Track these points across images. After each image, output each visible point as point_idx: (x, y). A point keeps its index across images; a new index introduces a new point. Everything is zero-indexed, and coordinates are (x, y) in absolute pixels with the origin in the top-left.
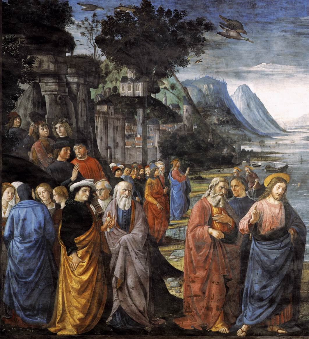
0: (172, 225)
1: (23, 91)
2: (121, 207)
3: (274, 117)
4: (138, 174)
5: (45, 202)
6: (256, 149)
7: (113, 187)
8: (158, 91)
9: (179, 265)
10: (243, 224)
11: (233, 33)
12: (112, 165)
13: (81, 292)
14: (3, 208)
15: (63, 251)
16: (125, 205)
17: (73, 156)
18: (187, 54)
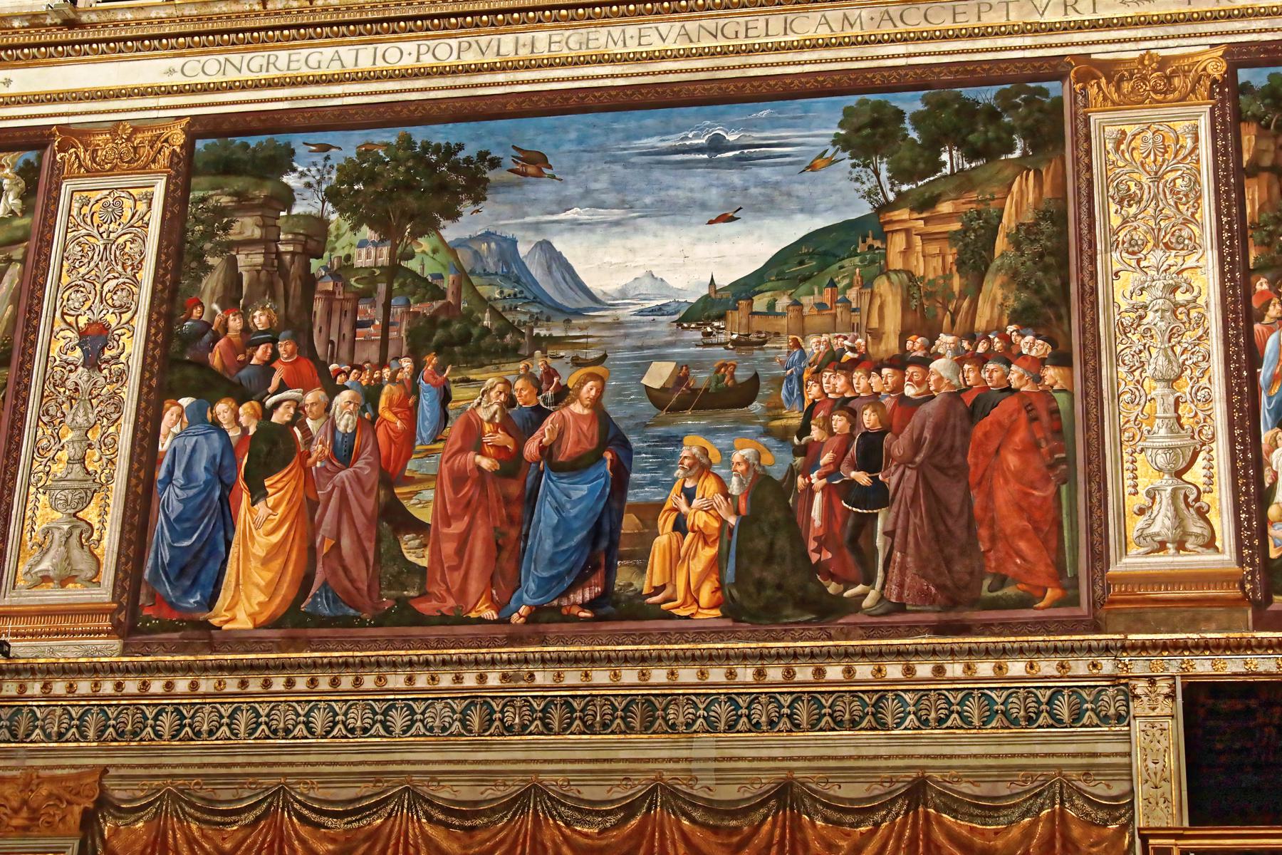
0: (418, 453)
1: (211, 268)
2: (341, 428)
3: (588, 285)
4: (371, 377)
5: (226, 427)
6: (557, 333)
7: (332, 399)
8: (411, 256)
9: (425, 515)
10: (531, 448)
11: (531, 169)
12: (333, 367)
13: (266, 562)
14: (161, 438)
15: (245, 498)
16: (347, 426)
17: (275, 355)
18: (460, 202)
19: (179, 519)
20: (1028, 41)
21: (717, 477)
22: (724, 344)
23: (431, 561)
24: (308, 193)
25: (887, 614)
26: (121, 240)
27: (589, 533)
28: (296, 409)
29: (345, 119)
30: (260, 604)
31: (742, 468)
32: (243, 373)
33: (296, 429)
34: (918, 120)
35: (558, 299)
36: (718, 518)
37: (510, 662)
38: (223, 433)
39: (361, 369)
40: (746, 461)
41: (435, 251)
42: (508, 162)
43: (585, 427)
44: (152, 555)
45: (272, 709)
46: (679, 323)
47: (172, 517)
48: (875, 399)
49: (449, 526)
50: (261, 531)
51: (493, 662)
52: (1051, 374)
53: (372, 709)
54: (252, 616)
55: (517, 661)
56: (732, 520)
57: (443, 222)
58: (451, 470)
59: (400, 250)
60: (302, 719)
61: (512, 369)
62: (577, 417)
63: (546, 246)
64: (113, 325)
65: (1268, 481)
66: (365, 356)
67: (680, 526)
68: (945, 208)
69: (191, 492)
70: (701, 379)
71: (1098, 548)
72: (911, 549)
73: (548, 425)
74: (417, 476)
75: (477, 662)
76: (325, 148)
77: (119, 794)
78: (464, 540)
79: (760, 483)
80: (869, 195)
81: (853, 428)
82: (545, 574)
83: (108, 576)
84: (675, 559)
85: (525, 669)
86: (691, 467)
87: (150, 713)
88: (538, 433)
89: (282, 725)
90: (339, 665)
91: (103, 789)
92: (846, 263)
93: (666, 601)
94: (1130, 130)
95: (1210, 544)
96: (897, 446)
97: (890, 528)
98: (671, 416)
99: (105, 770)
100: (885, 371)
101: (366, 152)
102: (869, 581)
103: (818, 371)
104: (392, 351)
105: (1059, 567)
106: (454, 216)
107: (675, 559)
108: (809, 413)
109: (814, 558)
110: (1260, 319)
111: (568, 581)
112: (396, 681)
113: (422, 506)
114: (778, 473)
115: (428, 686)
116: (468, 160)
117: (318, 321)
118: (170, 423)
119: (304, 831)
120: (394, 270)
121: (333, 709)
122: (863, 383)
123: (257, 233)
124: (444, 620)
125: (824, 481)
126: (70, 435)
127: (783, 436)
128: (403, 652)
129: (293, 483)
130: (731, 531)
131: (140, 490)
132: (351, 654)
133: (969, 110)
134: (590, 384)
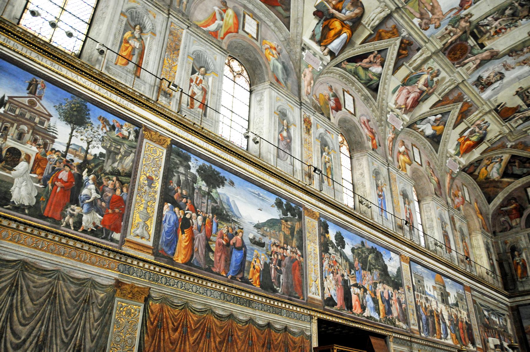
6: (236, 220)
9: (214, 249)
13: (184, 249)
19: (167, 232)
38: (176, 215)
46: (254, 227)
51: (227, 286)
52: (301, 258)
54: (182, 260)
63: (233, 201)
67: (254, 267)
70: (257, 239)
77: (153, 295)
83: (152, 239)
84: (254, 274)
85: (232, 289)
87: (160, 277)
91: (149, 293)
96: (283, 263)
99: (150, 288)
101: (204, 165)
114: (268, 263)
119: (191, 314)
123: (184, 172)
126: (144, 202)
127: (268, 255)
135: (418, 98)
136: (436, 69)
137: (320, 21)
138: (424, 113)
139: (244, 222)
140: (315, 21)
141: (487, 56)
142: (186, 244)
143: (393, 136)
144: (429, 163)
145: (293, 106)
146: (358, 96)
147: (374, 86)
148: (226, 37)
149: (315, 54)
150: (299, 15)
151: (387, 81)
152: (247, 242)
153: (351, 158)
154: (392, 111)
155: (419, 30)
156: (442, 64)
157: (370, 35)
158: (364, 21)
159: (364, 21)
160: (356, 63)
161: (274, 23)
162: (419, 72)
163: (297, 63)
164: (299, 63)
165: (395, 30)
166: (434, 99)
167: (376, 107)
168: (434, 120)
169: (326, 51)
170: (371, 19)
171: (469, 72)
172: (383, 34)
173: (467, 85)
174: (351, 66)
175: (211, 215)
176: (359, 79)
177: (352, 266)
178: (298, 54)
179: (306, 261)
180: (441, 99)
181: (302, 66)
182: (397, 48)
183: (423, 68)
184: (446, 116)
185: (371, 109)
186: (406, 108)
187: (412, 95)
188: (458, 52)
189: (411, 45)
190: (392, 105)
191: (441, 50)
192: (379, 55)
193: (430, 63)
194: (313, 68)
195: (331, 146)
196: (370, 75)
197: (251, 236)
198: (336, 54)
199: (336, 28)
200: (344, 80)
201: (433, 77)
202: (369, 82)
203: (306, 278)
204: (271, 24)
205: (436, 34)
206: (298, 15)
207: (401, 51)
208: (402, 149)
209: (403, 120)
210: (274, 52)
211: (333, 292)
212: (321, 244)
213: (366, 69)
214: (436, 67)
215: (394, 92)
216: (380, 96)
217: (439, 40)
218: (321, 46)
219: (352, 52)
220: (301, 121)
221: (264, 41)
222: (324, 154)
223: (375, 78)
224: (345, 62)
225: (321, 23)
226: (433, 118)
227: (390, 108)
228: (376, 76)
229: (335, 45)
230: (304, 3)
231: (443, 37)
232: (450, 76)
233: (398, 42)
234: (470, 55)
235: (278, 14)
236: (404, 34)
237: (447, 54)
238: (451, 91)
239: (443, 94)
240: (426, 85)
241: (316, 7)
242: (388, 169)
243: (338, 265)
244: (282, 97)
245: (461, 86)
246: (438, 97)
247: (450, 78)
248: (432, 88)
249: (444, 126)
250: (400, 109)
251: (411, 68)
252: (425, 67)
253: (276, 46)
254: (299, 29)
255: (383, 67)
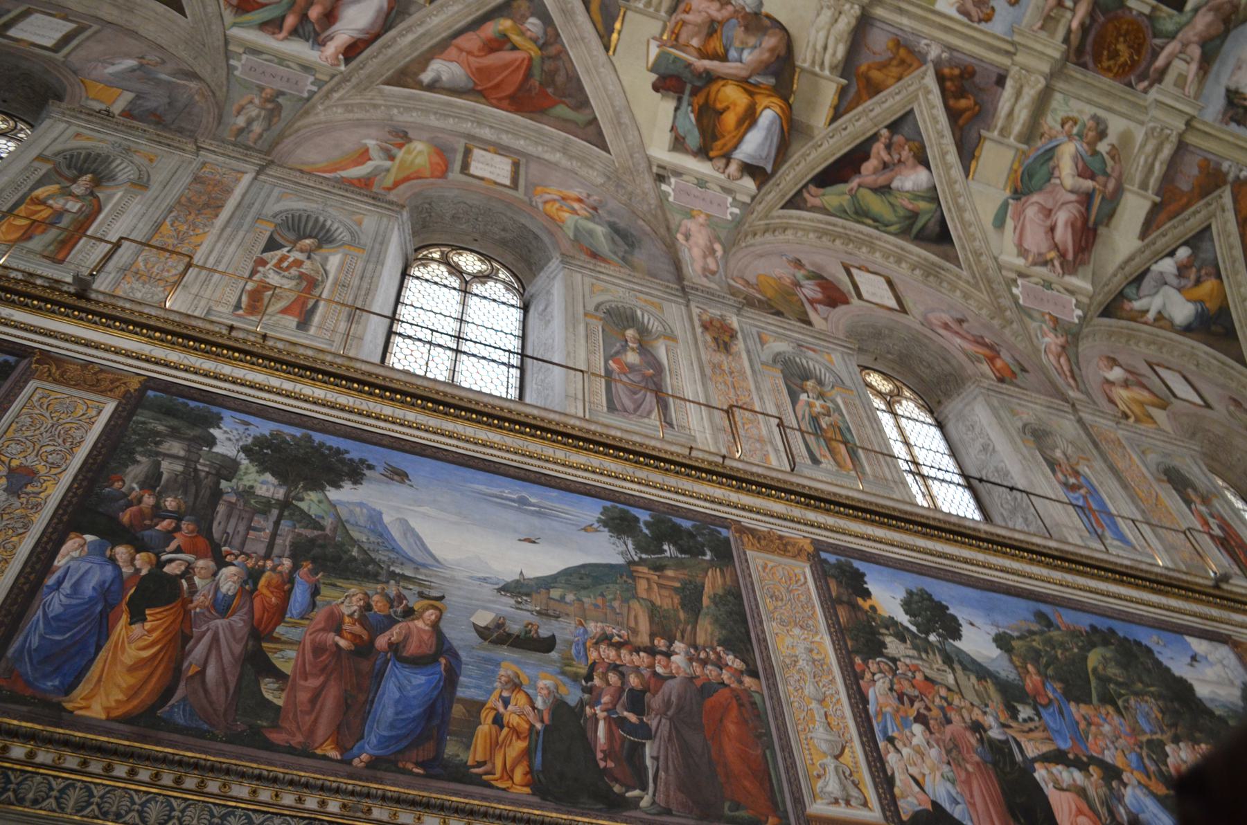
1: (138, 462)
2: (224, 589)
6: (408, 573)
8: (302, 500)
9: (287, 668)
10: (381, 642)
13: (131, 669)
14: (59, 557)
15: (125, 618)
19: (56, 618)
20: (707, 505)
21: (527, 695)
22: (531, 612)
23: (286, 702)
24: (228, 443)
25: (659, 814)
26: (68, 426)
27: (425, 711)
28: (187, 568)
29: (263, 412)
30: (118, 701)
31: (545, 692)
32: (147, 533)
33: (183, 581)
34: (647, 524)
35: (411, 554)
36: (528, 722)
37: (352, 793)
38: (117, 568)
39: (249, 556)
40: (548, 688)
41: (320, 502)
42: (380, 469)
43: (426, 637)
44: (21, 638)
45: (108, 792)
46: (499, 590)
47: (51, 615)
48: (637, 669)
49: (306, 679)
50: (133, 646)
51: (337, 791)
52: (748, 681)
53: (211, 812)
54: (107, 710)
55: (360, 794)
56: (539, 726)
57: (328, 488)
58: (313, 641)
59: (293, 494)
60: (136, 807)
61: (370, 587)
62: (419, 630)
63: (404, 523)
64: (42, 473)
65: (889, 773)
66: (254, 549)
67: (498, 721)
68: (670, 573)
69: (75, 602)
71: (797, 795)
72: (671, 771)
73: (396, 629)
74: (283, 638)
75: (322, 788)
76: (247, 424)
78: (316, 696)
79: (559, 707)
80: (622, 553)
81: (623, 683)
82: (385, 733)
84: (494, 745)
85: (366, 802)
86: (507, 683)
88: (388, 633)
89: (114, 809)
90: (188, 765)
92: (611, 586)
93: (487, 773)
94: (770, 564)
95: (865, 804)
96: (656, 702)
97: (655, 754)
98: (491, 647)
100: (642, 654)
102: (644, 788)
103: (597, 643)
104: (276, 551)
105: (775, 804)
106: (337, 486)
107: (494, 745)
108: (593, 667)
109: (602, 764)
110: (862, 678)
111: (405, 743)
112: (241, 790)
113: (285, 660)
115: (270, 801)
116: (351, 460)
117: (219, 518)
118: (71, 551)
120: (285, 505)
121: (170, 805)
122: (628, 657)
123: (182, 453)
124: (291, 750)
125: (605, 714)
127: (575, 678)
128: (255, 765)
129: (172, 618)
130: (538, 733)
131: (26, 587)
132: (204, 756)
133: (677, 529)
134: (431, 611)
135: (1085, 220)
136: (1086, 118)
137: (679, 100)
138: (1131, 259)
139: (452, 580)
140: (665, 107)
141: (1209, 25)
142: (146, 654)
143: (1061, 340)
144: (1235, 400)
145: (655, 300)
146: (901, 273)
147: (933, 227)
148: (402, 187)
149: (702, 183)
150: (616, 103)
151: (961, 200)
152: (459, 635)
153: (940, 425)
154: (1021, 275)
155: (968, 26)
156: (1095, 98)
157: (843, 92)
158: (804, 58)
159: (804, 61)
160: (845, 180)
161: (565, 150)
162: (1041, 145)
163: (655, 217)
164: (659, 212)
165: (902, 52)
166: (1134, 208)
167: (968, 282)
168: (1174, 271)
169: (733, 168)
170: (819, 47)
171: (1191, 89)
172: (876, 75)
173: (1207, 129)
174: (835, 196)
175: (287, 563)
176: (879, 223)
177: (1012, 695)
178: (652, 194)
179: (773, 687)
180: (1158, 199)
181: (669, 216)
182: (936, 97)
183: (1046, 128)
184: (1206, 245)
185: (958, 293)
186: (1063, 255)
187: (1062, 217)
188: (1121, 47)
189: (973, 74)
190: (1010, 257)
191: (1066, 58)
192: (897, 138)
193: (1060, 107)
194: (708, 216)
195: (828, 378)
196: (906, 203)
197: (484, 618)
198: (769, 169)
199: (735, 105)
200: (838, 242)
201: (1092, 144)
202: (912, 225)
203: (787, 748)
204: (557, 157)
205: (1025, 21)
206: (613, 107)
207: (951, 102)
208: (1116, 374)
209: (1072, 292)
210: (576, 206)
211: (940, 790)
212: (838, 633)
213: (884, 190)
214: (1085, 112)
215: (999, 223)
216: (963, 248)
217: (1043, 35)
218: (710, 159)
219: (814, 155)
220: (693, 328)
221: (539, 189)
222: (803, 397)
223: (922, 205)
224: (812, 188)
225: (685, 103)
226: (1167, 266)
227: (1011, 270)
228: (923, 198)
229: (754, 144)
230: (616, 71)
231: (1048, 22)
232: (1142, 123)
233: (931, 81)
234: (1158, 41)
235: (564, 124)
236: (934, 52)
237: (1091, 65)
238: (1173, 164)
239: (1153, 182)
240: (1085, 172)
241: (653, 69)
242: (1080, 421)
243: (943, 692)
244: (614, 284)
245: (1191, 139)
246: (1145, 197)
247: (1143, 130)
248: (1108, 176)
249: (1218, 276)
250: (1045, 263)
251: (1012, 140)
252: (1051, 122)
253: (583, 196)
254: (630, 137)
255: (928, 167)
